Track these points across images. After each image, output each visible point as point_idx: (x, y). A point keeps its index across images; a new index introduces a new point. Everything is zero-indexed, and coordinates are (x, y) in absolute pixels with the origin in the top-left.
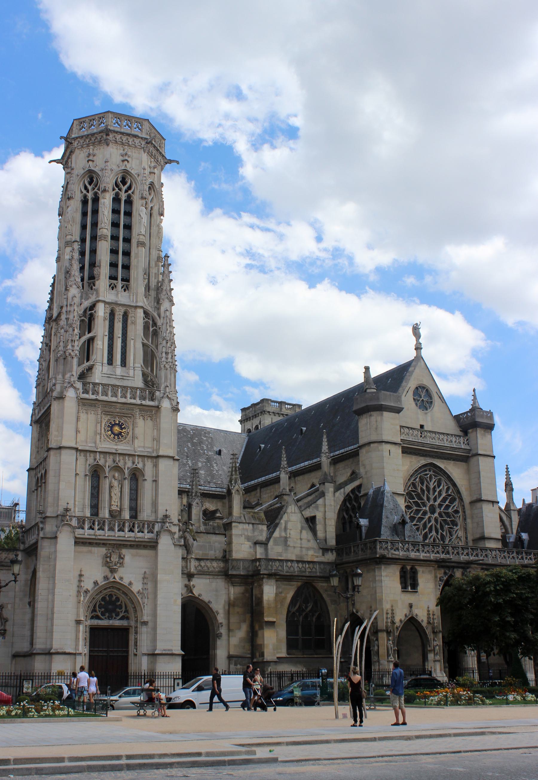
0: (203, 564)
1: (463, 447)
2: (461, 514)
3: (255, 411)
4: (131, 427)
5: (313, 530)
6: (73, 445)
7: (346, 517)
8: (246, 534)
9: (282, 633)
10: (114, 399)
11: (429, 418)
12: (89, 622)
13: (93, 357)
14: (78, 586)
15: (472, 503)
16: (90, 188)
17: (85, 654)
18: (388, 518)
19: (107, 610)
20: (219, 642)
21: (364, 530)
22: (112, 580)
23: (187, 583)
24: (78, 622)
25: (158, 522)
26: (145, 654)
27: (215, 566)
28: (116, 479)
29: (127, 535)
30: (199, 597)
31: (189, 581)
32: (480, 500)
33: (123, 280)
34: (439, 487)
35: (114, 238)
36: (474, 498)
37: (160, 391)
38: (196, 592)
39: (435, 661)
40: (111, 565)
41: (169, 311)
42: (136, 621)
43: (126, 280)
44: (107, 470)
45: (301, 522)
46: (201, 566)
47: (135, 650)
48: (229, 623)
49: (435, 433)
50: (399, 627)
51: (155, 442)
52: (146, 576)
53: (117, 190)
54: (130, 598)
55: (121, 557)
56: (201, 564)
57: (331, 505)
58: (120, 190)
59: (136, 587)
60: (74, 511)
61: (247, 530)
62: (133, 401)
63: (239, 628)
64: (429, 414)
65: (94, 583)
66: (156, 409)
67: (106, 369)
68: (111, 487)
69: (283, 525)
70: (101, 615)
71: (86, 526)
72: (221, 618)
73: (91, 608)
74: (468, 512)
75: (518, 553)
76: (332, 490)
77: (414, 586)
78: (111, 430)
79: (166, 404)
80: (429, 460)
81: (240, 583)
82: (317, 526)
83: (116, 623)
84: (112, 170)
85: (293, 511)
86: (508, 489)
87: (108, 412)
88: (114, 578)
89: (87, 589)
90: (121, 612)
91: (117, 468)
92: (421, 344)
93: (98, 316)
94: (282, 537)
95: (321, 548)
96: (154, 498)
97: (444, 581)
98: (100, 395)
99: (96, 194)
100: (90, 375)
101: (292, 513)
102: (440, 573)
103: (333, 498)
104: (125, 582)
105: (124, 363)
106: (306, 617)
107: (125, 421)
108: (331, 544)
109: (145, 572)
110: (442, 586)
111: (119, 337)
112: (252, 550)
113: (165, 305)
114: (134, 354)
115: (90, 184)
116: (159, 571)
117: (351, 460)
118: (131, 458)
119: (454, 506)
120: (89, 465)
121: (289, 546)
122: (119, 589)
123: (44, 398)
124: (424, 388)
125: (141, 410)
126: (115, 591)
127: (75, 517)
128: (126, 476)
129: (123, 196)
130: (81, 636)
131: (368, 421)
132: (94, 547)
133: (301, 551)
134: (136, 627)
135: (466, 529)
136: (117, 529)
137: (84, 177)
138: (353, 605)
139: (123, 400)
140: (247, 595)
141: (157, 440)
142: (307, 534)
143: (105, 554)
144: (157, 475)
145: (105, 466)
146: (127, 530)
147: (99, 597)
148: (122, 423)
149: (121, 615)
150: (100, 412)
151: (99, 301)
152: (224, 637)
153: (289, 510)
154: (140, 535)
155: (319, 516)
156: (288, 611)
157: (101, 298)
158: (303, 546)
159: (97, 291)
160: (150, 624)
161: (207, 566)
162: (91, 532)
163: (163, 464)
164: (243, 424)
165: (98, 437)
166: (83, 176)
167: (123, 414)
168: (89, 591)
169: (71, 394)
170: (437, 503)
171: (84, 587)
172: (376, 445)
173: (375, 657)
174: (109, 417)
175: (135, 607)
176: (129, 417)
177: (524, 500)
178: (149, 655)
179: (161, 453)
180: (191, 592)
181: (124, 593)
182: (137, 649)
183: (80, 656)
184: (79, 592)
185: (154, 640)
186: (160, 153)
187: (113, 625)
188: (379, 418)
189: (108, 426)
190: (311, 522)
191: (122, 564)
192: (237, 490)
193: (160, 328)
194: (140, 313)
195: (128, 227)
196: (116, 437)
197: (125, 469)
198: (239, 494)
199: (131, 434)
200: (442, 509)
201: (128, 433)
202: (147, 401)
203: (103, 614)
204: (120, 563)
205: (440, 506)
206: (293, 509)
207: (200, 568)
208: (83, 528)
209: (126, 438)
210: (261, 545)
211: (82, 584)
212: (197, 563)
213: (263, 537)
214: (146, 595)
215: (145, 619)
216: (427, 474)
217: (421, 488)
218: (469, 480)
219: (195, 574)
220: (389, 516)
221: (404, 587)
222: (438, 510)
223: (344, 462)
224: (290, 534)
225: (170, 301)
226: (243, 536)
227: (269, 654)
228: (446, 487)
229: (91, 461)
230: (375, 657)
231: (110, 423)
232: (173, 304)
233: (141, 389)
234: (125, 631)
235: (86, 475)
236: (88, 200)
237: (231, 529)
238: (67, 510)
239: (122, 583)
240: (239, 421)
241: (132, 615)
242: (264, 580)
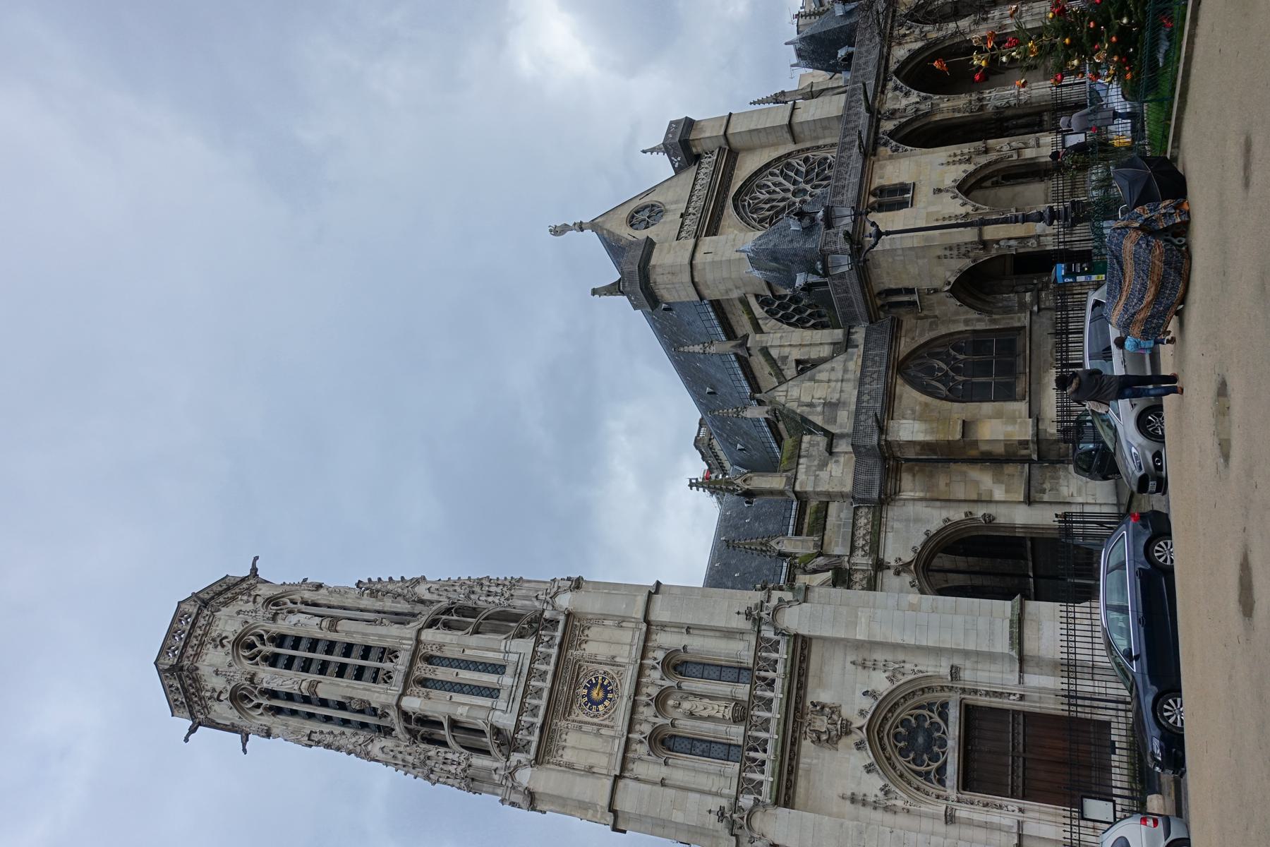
0: (861, 542)
1: (715, 158)
3: (710, 457)
4: (596, 666)
5: (815, 364)
6: (608, 783)
7: (812, 322)
8: (814, 468)
9: (987, 407)
10: (545, 695)
11: (673, 207)
12: (952, 792)
14: (875, 808)
16: (256, 701)
17: (1021, 810)
18: (792, 240)
19: (928, 748)
20: (1001, 520)
22: (863, 735)
23: (892, 571)
24: (950, 818)
25: (759, 631)
26: (1021, 677)
27: (866, 521)
28: (680, 704)
29: (777, 695)
30: (918, 551)
31: (889, 568)
32: (790, 125)
33: (381, 660)
34: (769, 187)
35: (323, 668)
36: (788, 136)
37: (544, 610)
38: (908, 557)
39: (1038, 145)
40: (834, 733)
42: (951, 689)
44: (660, 721)
45: (802, 382)
46: (864, 545)
47: (1012, 697)
48: (965, 501)
49: (691, 196)
50: (974, 206)
51: (624, 624)
52: (860, 660)
54: (903, 697)
55: (821, 708)
56: (861, 545)
57: (781, 337)
58: (260, 652)
59: (881, 683)
60: (728, 797)
61: (808, 468)
62: (553, 660)
63: (977, 483)
64: (667, 207)
65: (868, 772)
66: (571, 618)
67: (501, 704)
68: (691, 715)
69: (805, 408)
70: (937, 762)
71: (757, 777)
72: (957, 514)
73: (918, 781)
74: (808, 145)
76: (758, 336)
77: (903, 188)
78: (598, 703)
79: (565, 601)
80: (730, 201)
81: (896, 480)
82: (812, 357)
83: (953, 731)
84: (230, 665)
85: (785, 393)
87: (566, 708)
88: (860, 728)
89: (882, 790)
90: (931, 718)
91: (660, 702)
92: (575, 224)
94: (823, 412)
95: (846, 351)
96: (718, 634)
97: (899, 145)
98: (535, 720)
100: (508, 732)
101: (786, 396)
102: (884, 151)
103: (771, 335)
104: (869, 704)
105: (498, 669)
106: (956, 370)
107: (586, 675)
108: (841, 336)
109: (853, 663)
110: (906, 147)
111: (457, 674)
112: (842, 459)
113: (422, 590)
114: (487, 650)
116: (850, 636)
117: (729, 316)
118: (647, 672)
119: (798, 164)
120: (649, 755)
121: (838, 400)
122: (885, 718)
124: (633, 217)
125: (570, 646)
126: (887, 727)
127: (737, 799)
129: (270, 649)
130: (979, 815)
131: (663, 286)
132: (798, 763)
133: (848, 380)
134: (964, 690)
136: (766, 714)
137: (243, 709)
138: (936, 291)
140: (917, 468)
141: (621, 622)
142: (823, 373)
143: (813, 742)
144: (678, 626)
145: (655, 723)
146: (768, 694)
147: (900, 762)
148: (588, 682)
149: (937, 719)
150: (564, 723)
151: (398, 706)
152: (991, 510)
153: (782, 400)
154: (780, 667)
155: (796, 354)
156: (946, 399)
158: (841, 378)
159: (385, 706)
160: (957, 661)
161: (864, 535)
162: (768, 767)
163: (660, 613)
165: (603, 731)
166: (240, 710)
167: (573, 678)
168: (885, 786)
170: (792, 188)
171: (876, 796)
172: (695, 274)
173: (1030, 244)
174: (574, 707)
175: (923, 690)
176: (579, 668)
177: (792, 66)
178: (1021, 671)
179: (639, 615)
180: (910, 563)
181: (892, 710)
182: (1010, 694)
183: (1025, 826)
184: (886, 809)
185: (991, 657)
186: (236, 584)
187: (957, 739)
188: (659, 270)
189: (589, 709)
190: (805, 367)
191: (835, 710)
192: (745, 481)
193: (453, 603)
194: (429, 635)
195: (314, 644)
196: (610, 696)
197: (662, 686)
198: (751, 478)
199: (607, 668)
200: (801, 180)
201: (605, 673)
202: (556, 634)
203: (934, 758)
204: (833, 712)
205: (795, 183)
206: (781, 394)
207: (867, 548)
208: (761, 783)
209: (613, 678)
210: (834, 445)
211: (871, 799)
212: (860, 552)
213: (821, 441)
214: (897, 666)
215: (945, 671)
216: (749, 203)
218: (763, 147)
219: (878, 557)
220: (789, 238)
221: (903, 205)
222: (803, 186)
223: (735, 328)
224: (820, 399)
225: (419, 583)
226: (817, 473)
227: (1023, 431)
228: (770, 177)
229: (642, 749)
230: (1030, 244)
231: (586, 705)
232: (424, 578)
233: (537, 644)
234: (969, 712)
235: (666, 763)
237: (806, 492)
238: (721, 814)
239: (871, 712)
241: (943, 696)
242: (889, 439)
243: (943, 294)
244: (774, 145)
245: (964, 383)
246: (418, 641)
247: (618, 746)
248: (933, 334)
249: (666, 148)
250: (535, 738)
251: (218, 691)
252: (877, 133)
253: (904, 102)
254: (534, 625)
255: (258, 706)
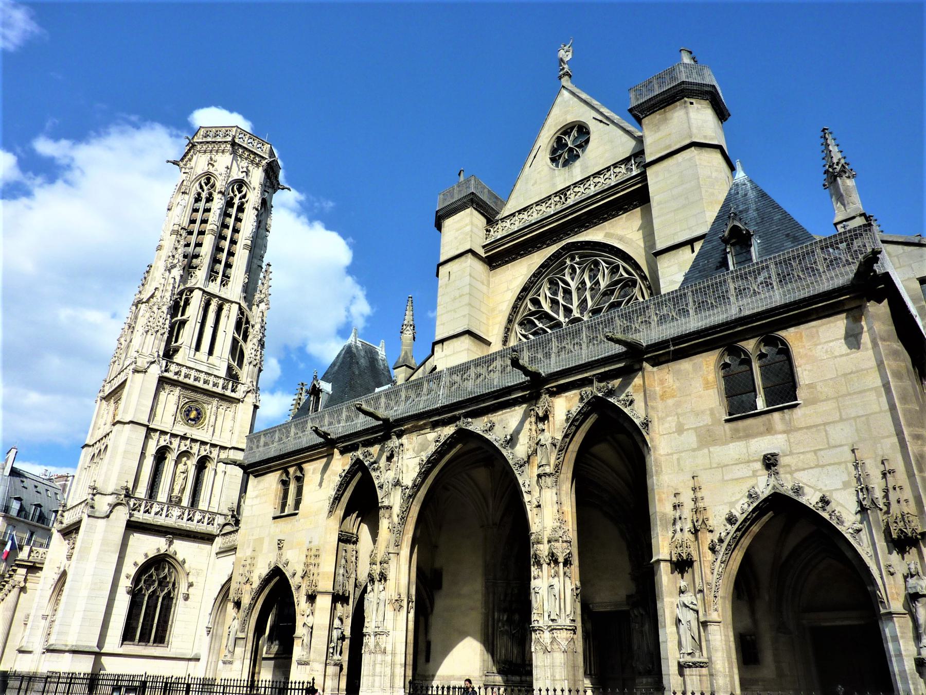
16: (205, 188)
29: (184, 524)
43: (226, 277)
53: (232, 194)
58: (235, 195)
99: (210, 194)
105: (211, 352)
115: (206, 184)
123: (119, 374)
166: (201, 176)
193: (253, 326)
194: (235, 308)
246: (232, 302)
251: (214, 164)
254: (232, 376)
255: (201, 187)
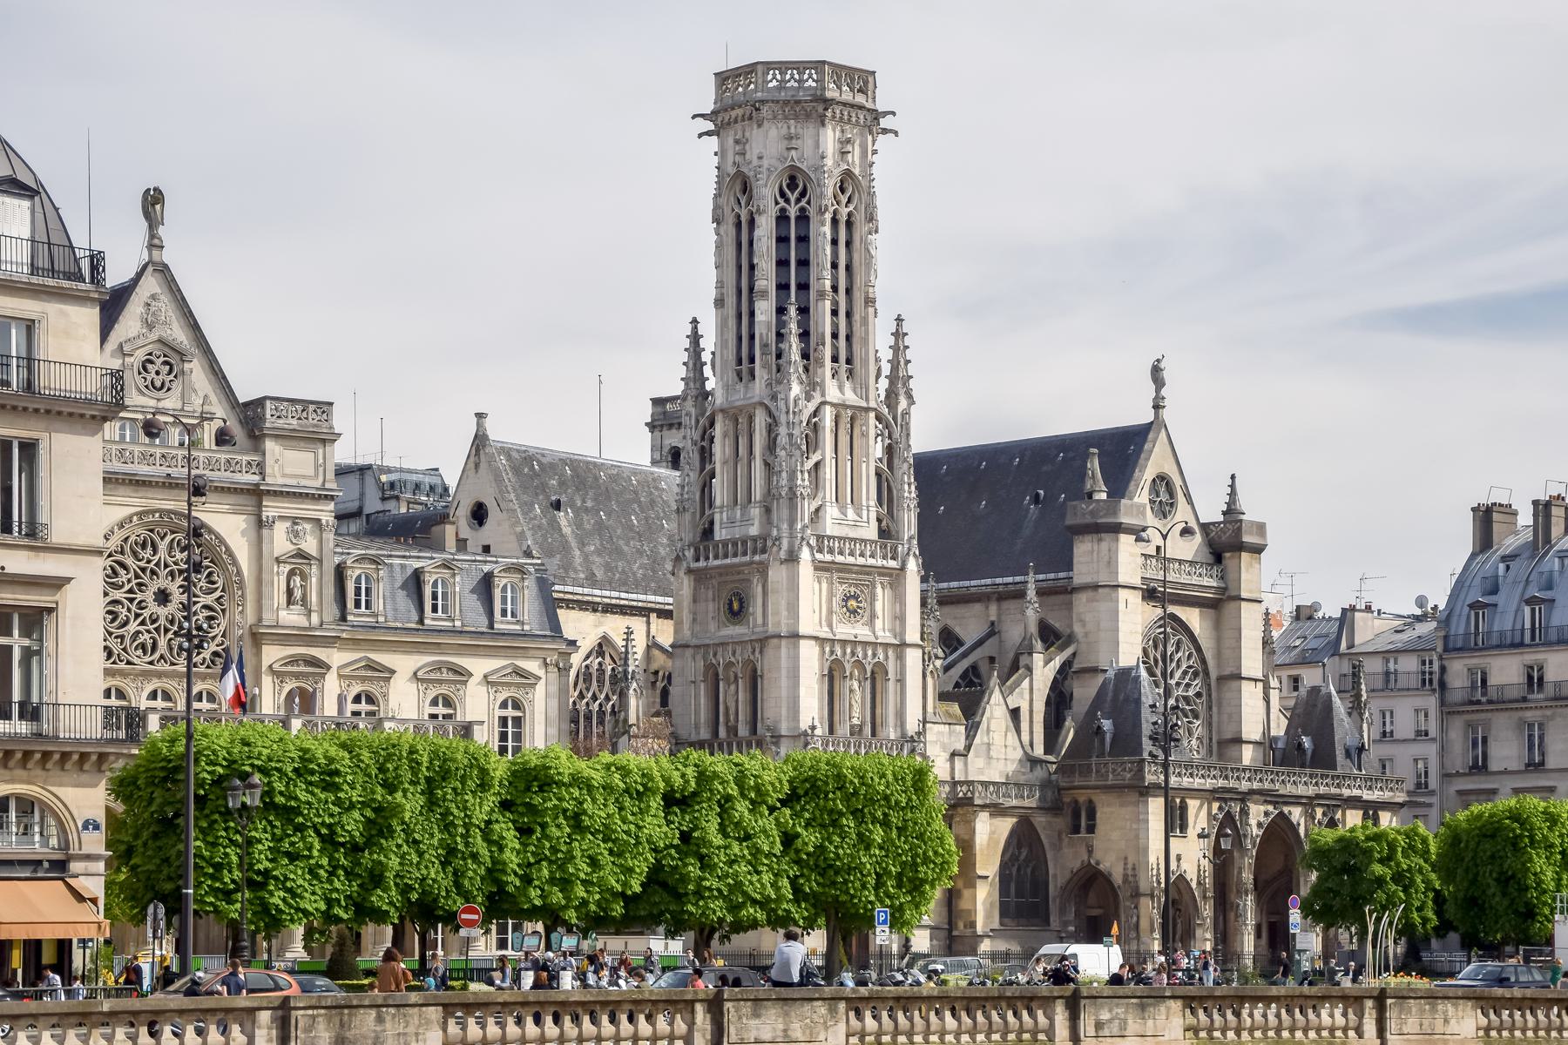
2: (1204, 698)
13: (820, 495)
15: (1221, 679)
16: (793, 200)
21: (1108, 737)
41: (906, 413)
44: (848, 667)
68: (851, 691)
75: (1311, 776)
86: (1267, 650)
91: (859, 664)
93: (824, 428)
107: (862, 591)
113: (903, 403)
128: (869, 675)
131: (1096, 547)
135: (1210, 724)
139: (861, 561)
141: (900, 618)
142: (1012, 737)
151: (824, 403)
153: (992, 701)
157: (828, 399)
164: (657, 433)
169: (805, 554)
172: (1106, 590)
213: (960, 745)
217: (1156, 661)
218: (1219, 640)
232: (913, 403)
236: (788, 218)
240: (647, 424)
243: (1086, 858)
244: (1219, 655)
245: (1011, 874)
247: (824, 632)
248: (1047, 846)
249: (1231, 511)
250: (828, 558)
252: (1231, 799)
253: (1253, 822)
